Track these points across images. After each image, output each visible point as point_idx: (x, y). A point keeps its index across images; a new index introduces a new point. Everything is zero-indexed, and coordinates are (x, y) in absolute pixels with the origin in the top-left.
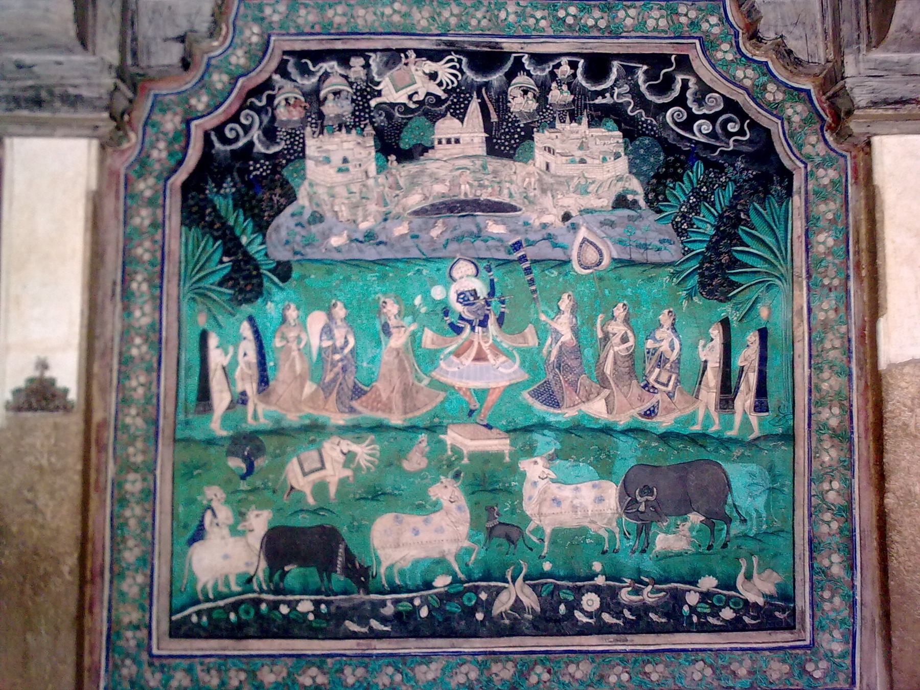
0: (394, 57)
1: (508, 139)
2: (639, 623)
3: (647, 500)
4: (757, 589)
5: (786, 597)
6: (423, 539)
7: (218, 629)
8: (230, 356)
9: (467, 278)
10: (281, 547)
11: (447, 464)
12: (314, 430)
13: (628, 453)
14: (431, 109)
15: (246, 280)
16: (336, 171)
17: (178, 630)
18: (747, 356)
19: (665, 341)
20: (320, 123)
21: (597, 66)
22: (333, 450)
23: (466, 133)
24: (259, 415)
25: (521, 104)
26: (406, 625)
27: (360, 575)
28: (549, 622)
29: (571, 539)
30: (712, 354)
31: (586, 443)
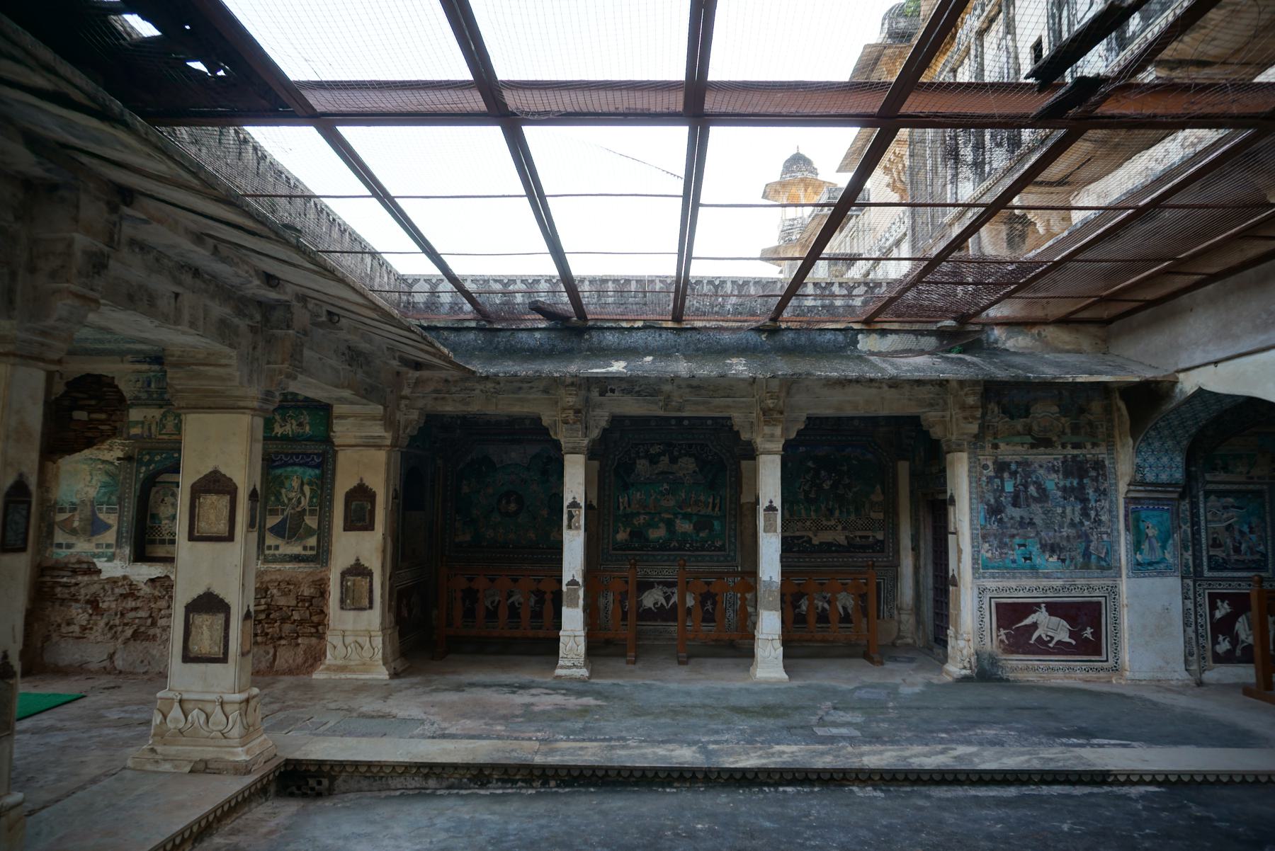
0: (652, 445)
1: (673, 460)
2: (697, 550)
3: (698, 528)
4: (718, 544)
5: (724, 545)
6: (657, 533)
7: (621, 549)
8: (623, 500)
9: (666, 486)
10: (631, 534)
11: (662, 520)
12: (639, 514)
13: (695, 519)
14: (660, 454)
15: (626, 487)
16: (642, 465)
17: (614, 549)
18: (718, 501)
19: (702, 498)
20: (639, 458)
21: (690, 446)
22: (642, 517)
23: (665, 459)
24: (629, 510)
25: (676, 453)
26: (654, 549)
27: (647, 540)
28: (679, 549)
29: (684, 534)
30: (711, 500)
31: (687, 517)
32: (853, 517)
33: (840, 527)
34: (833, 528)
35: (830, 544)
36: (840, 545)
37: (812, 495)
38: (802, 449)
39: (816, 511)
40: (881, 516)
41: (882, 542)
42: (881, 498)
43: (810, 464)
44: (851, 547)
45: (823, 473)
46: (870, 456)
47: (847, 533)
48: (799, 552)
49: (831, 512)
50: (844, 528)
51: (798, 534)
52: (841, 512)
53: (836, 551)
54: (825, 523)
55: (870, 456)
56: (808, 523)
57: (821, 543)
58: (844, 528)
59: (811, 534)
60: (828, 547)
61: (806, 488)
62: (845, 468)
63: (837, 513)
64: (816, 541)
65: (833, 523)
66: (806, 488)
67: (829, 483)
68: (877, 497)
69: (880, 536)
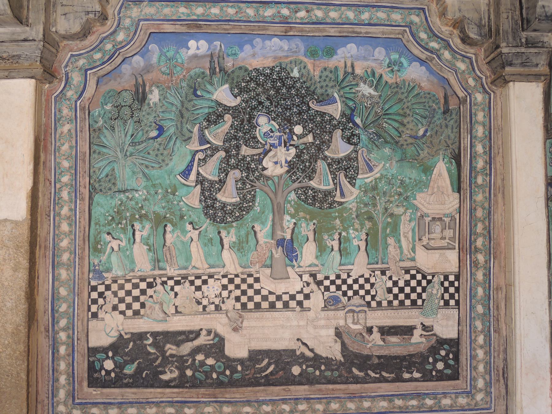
32: (359, 266)
33: (317, 299)
34: (297, 302)
35: (282, 359)
36: (317, 360)
37: (228, 196)
38: (197, 47)
39: (239, 247)
40: (449, 261)
41: (454, 344)
42: (451, 202)
43: (223, 95)
44: (355, 366)
45: (264, 124)
46: (414, 72)
47: (339, 318)
48: (181, 382)
49: (289, 249)
50: (331, 304)
51: (177, 324)
52: (322, 249)
53: (305, 379)
54: (267, 285)
55: (414, 72)
56: (213, 289)
57: (256, 356)
58: (331, 304)
59: (220, 324)
60: (275, 369)
61: (210, 171)
62: (335, 110)
63: (308, 253)
64: (237, 348)
65: (294, 285)
66: (210, 171)
67: (285, 155)
68: (438, 197)
69: (446, 326)
